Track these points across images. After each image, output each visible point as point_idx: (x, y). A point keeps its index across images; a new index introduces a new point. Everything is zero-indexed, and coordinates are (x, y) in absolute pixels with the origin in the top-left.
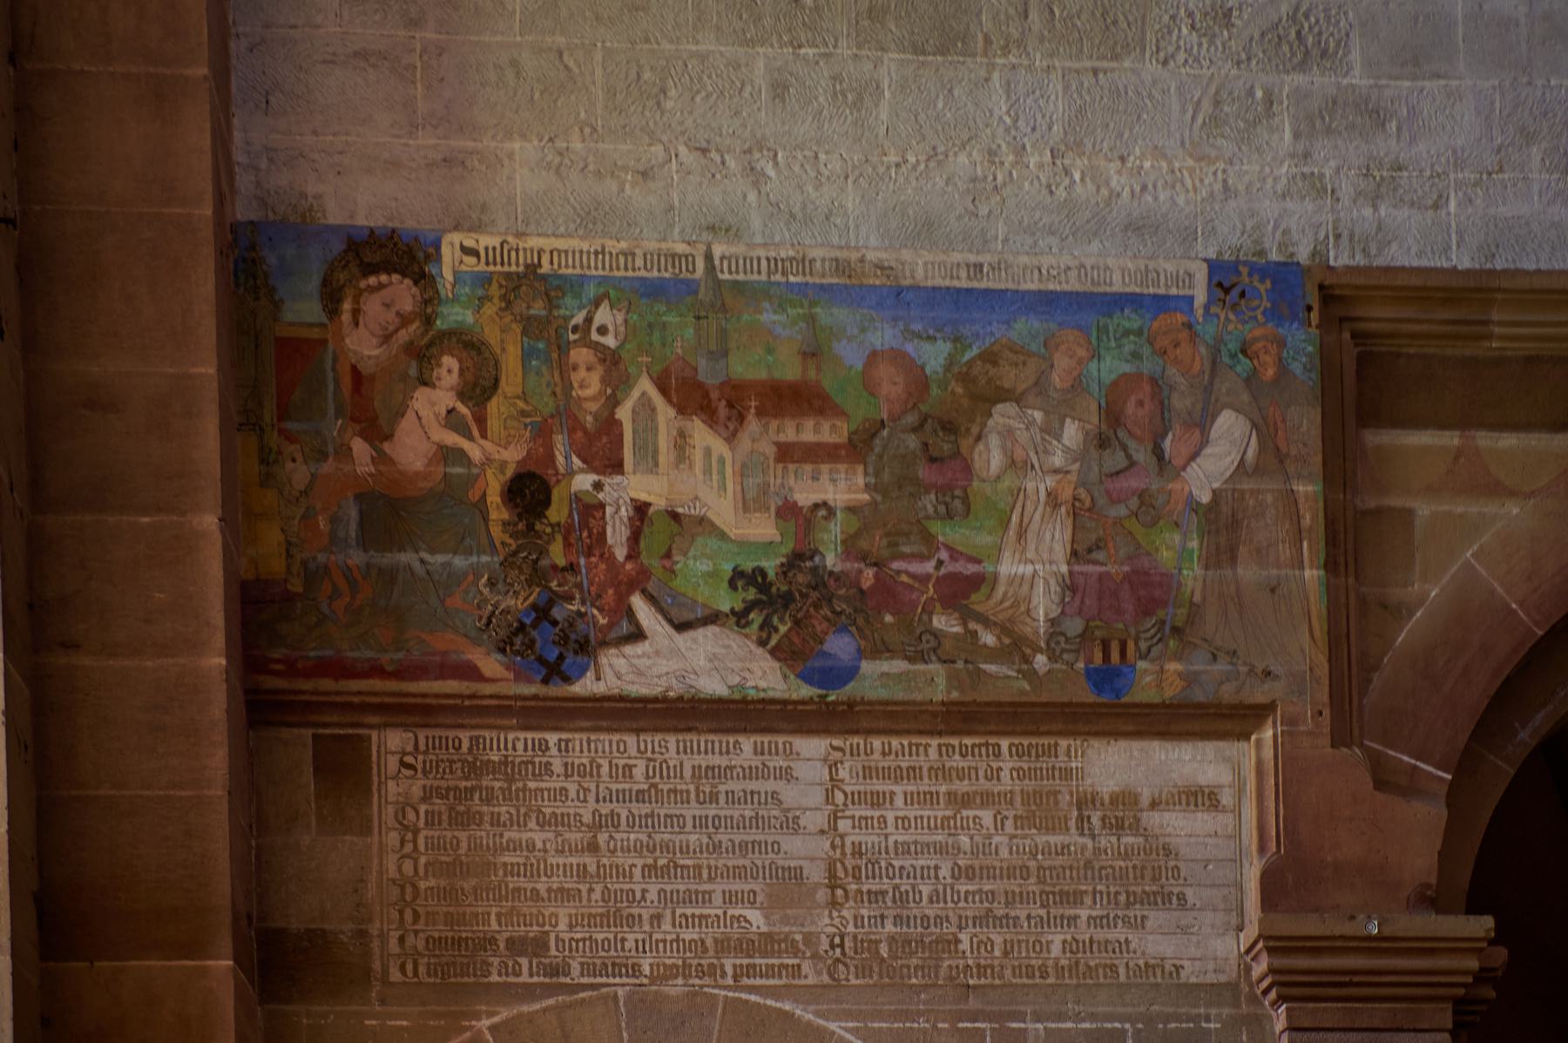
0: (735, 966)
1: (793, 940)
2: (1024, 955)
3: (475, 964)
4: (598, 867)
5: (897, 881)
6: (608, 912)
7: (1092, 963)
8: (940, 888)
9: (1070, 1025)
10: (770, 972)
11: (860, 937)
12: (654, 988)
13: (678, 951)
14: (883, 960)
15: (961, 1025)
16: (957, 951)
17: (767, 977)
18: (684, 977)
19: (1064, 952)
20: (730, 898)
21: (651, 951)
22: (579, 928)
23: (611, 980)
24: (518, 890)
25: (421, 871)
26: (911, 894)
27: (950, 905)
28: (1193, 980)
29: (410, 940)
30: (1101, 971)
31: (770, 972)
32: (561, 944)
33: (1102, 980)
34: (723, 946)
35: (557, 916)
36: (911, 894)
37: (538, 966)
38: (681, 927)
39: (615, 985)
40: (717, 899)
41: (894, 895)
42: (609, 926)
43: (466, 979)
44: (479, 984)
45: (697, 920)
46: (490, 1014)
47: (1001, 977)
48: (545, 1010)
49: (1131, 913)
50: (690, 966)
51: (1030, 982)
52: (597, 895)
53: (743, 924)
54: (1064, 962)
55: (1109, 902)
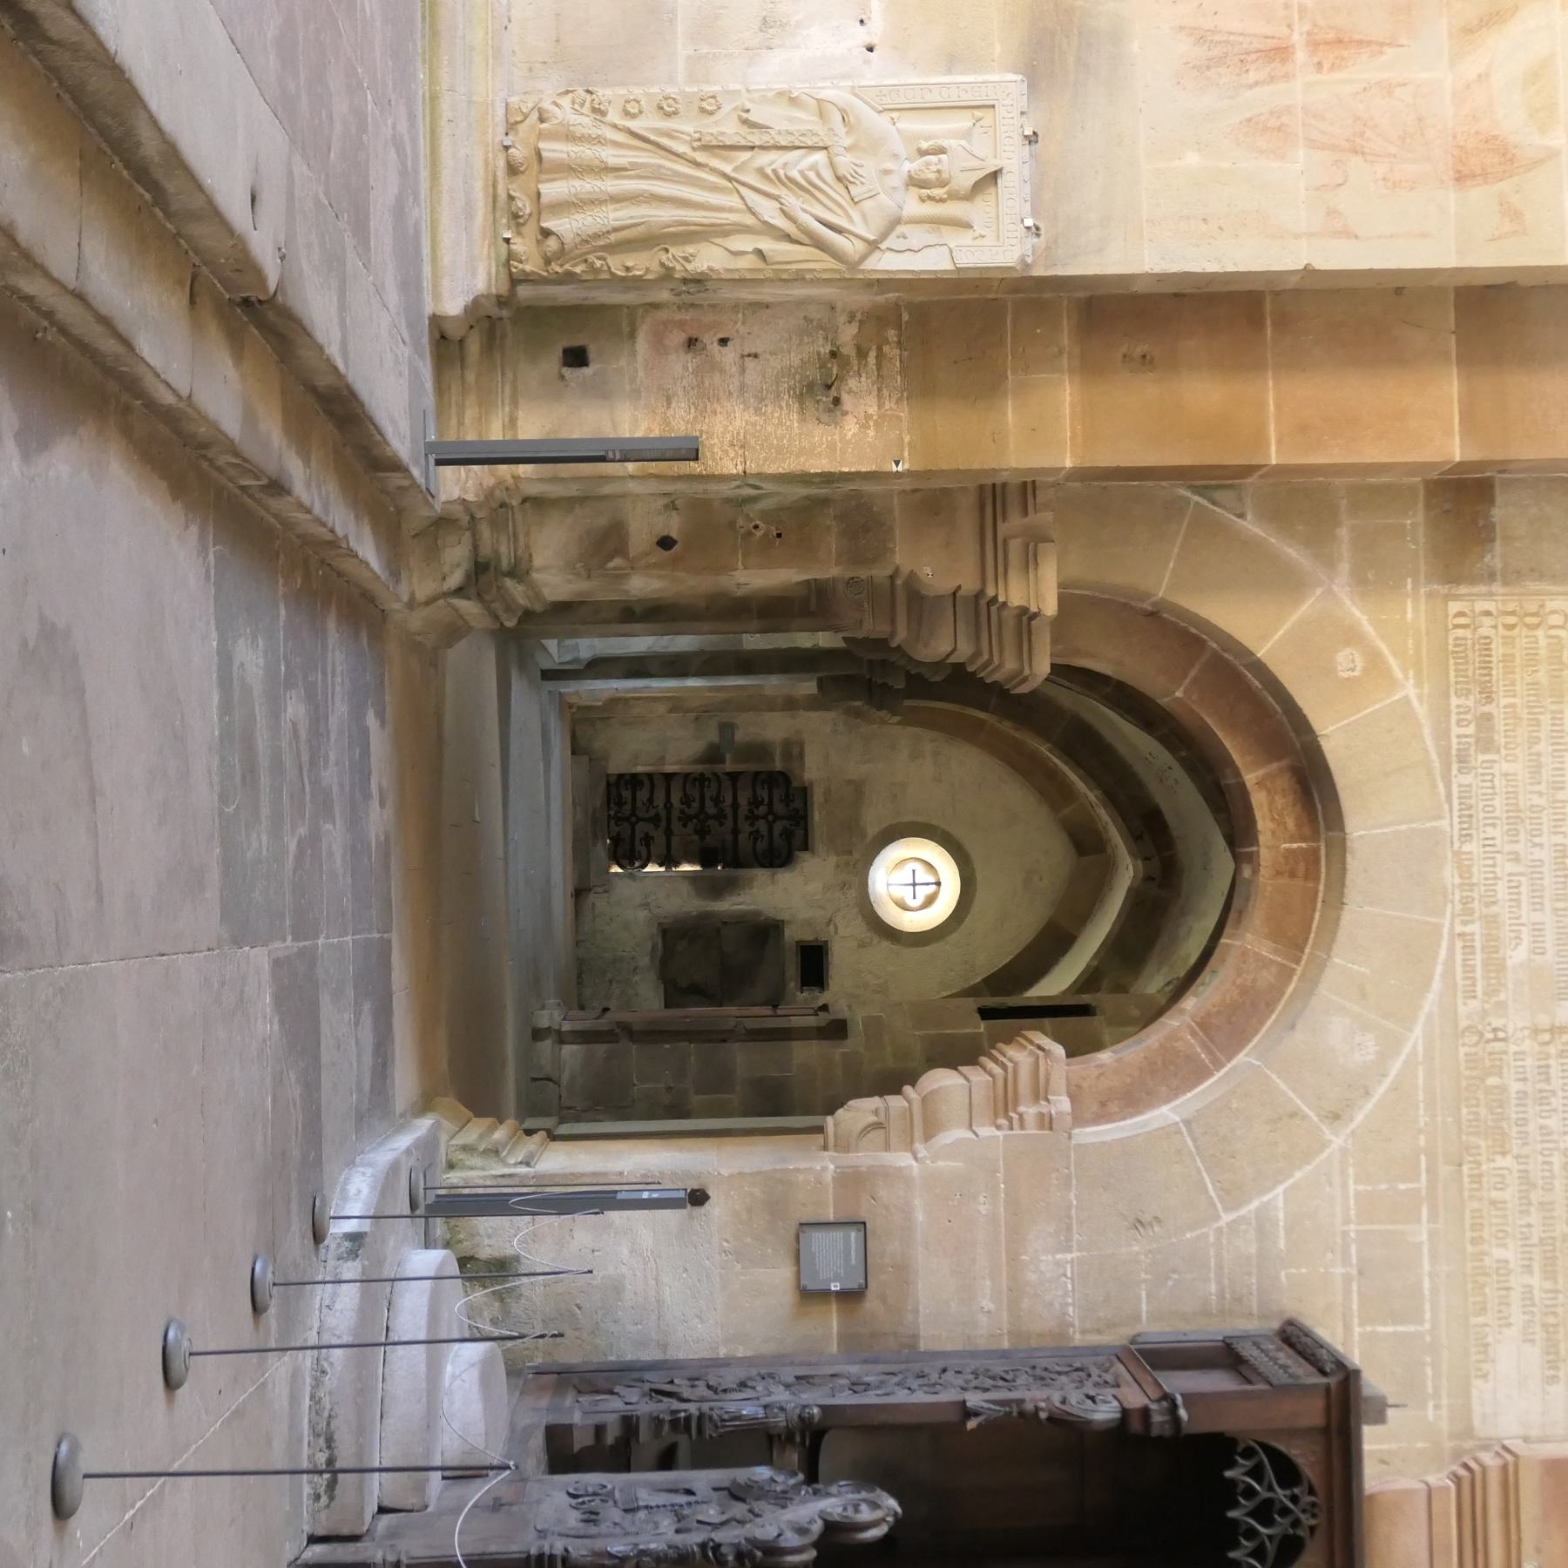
0: (1472, 934)
1: (1499, 991)
2: (1494, 1221)
3: (1467, 683)
4: (1563, 801)
5: (1560, 1093)
6: (1520, 811)
7: (1487, 1290)
8: (1555, 1137)
9: (1426, 1266)
10: (1469, 969)
11: (1504, 1057)
12: (1450, 855)
13: (1486, 879)
14: (1483, 1080)
15: (1423, 1158)
16: (1494, 1153)
17: (1464, 966)
18: (1462, 884)
19: (1498, 1261)
20: (1538, 929)
21: (1485, 852)
22: (1504, 782)
23: (1456, 814)
24: (1538, 724)
25: (1554, 632)
26: (1547, 1108)
27: (1539, 1147)
28: (1474, 1392)
29: (1487, 621)
30: (1479, 1299)
31: (1469, 969)
32: (1489, 765)
33: (1471, 1299)
34: (1491, 921)
35: (1514, 761)
36: (1547, 1108)
37: (1467, 743)
38: (1509, 881)
39: (1451, 817)
40: (1537, 917)
41: (1545, 1091)
42: (1508, 811)
43: (1452, 674)
44: (1448, 687)
45: (1516, 897)
46: (1420, 697)
47: (1471, 1197)
48: (1425, 750)
49: (1538, 1328)
50: (1472, 891)
51: (1467, 1226)
52: (1536, 800)
53: (1514, 942)
54: (1486, 1258)
55: (1546, 1306)
